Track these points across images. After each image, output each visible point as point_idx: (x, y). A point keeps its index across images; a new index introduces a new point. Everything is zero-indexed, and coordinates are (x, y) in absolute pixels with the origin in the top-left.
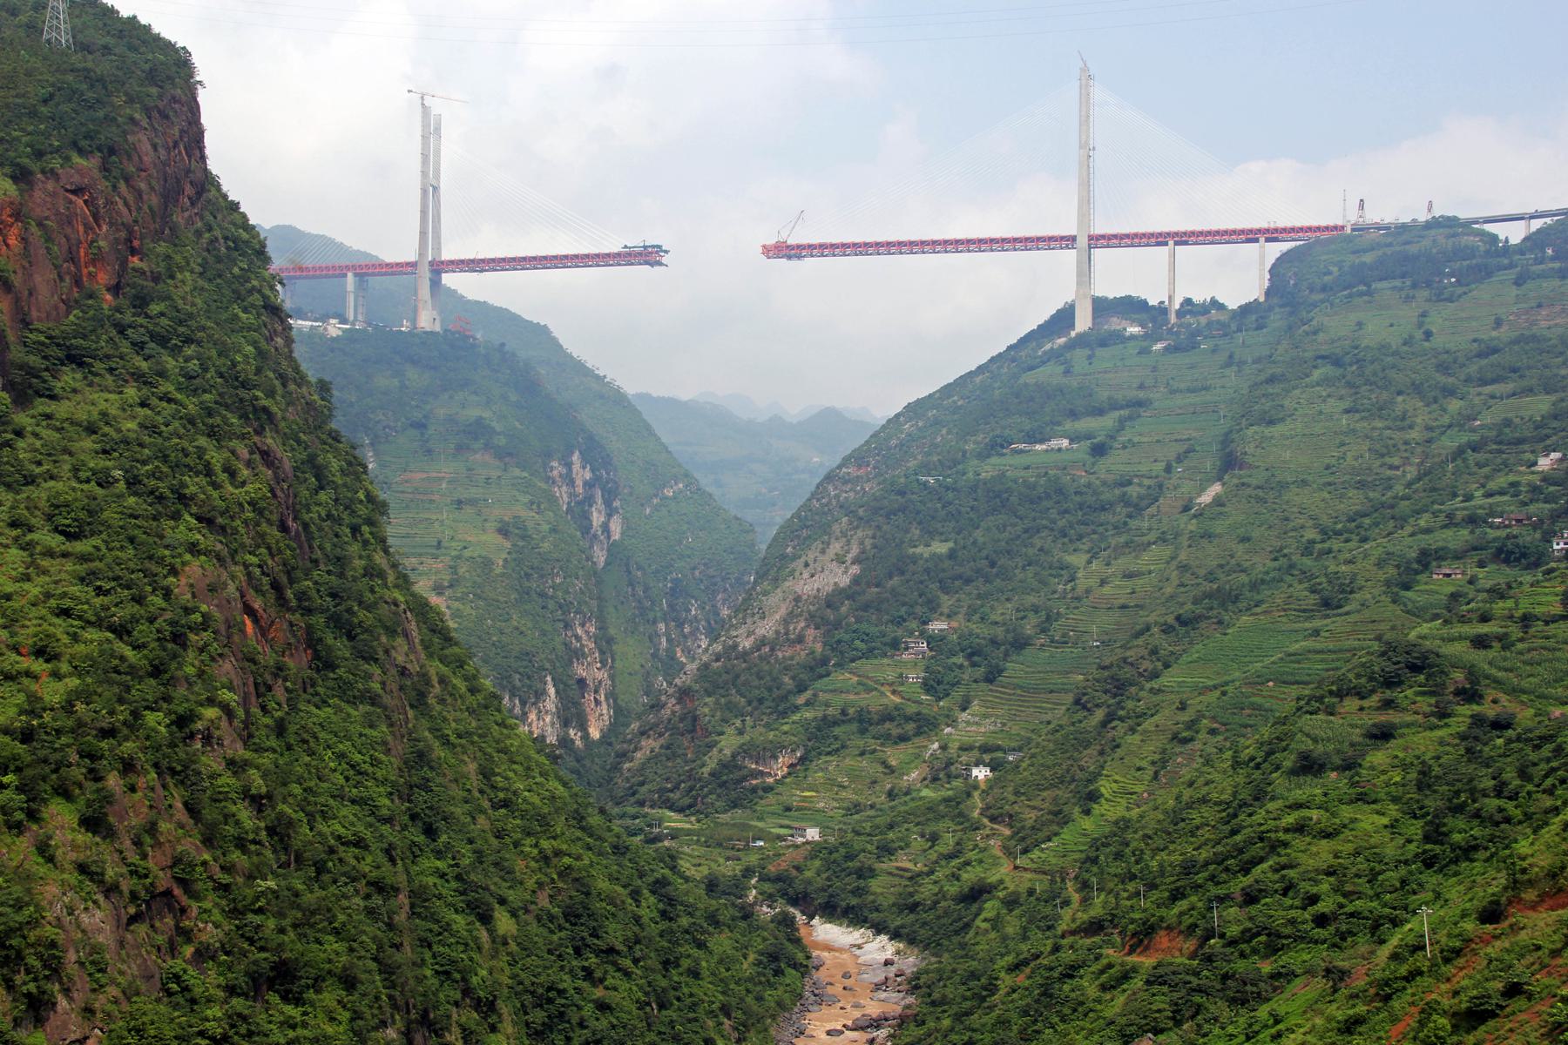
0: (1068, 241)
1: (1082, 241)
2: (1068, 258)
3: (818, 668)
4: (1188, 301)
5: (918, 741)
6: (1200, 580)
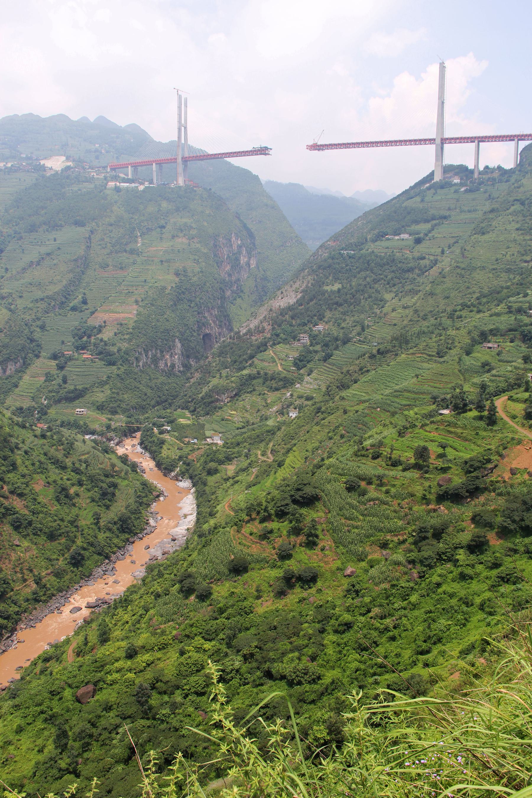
0: (431, 141)
1: (438, 141)
2: (431, 149)
3: (263, 347)
4: (487, 167)
5: (283, 391)
6: (419, 319)
